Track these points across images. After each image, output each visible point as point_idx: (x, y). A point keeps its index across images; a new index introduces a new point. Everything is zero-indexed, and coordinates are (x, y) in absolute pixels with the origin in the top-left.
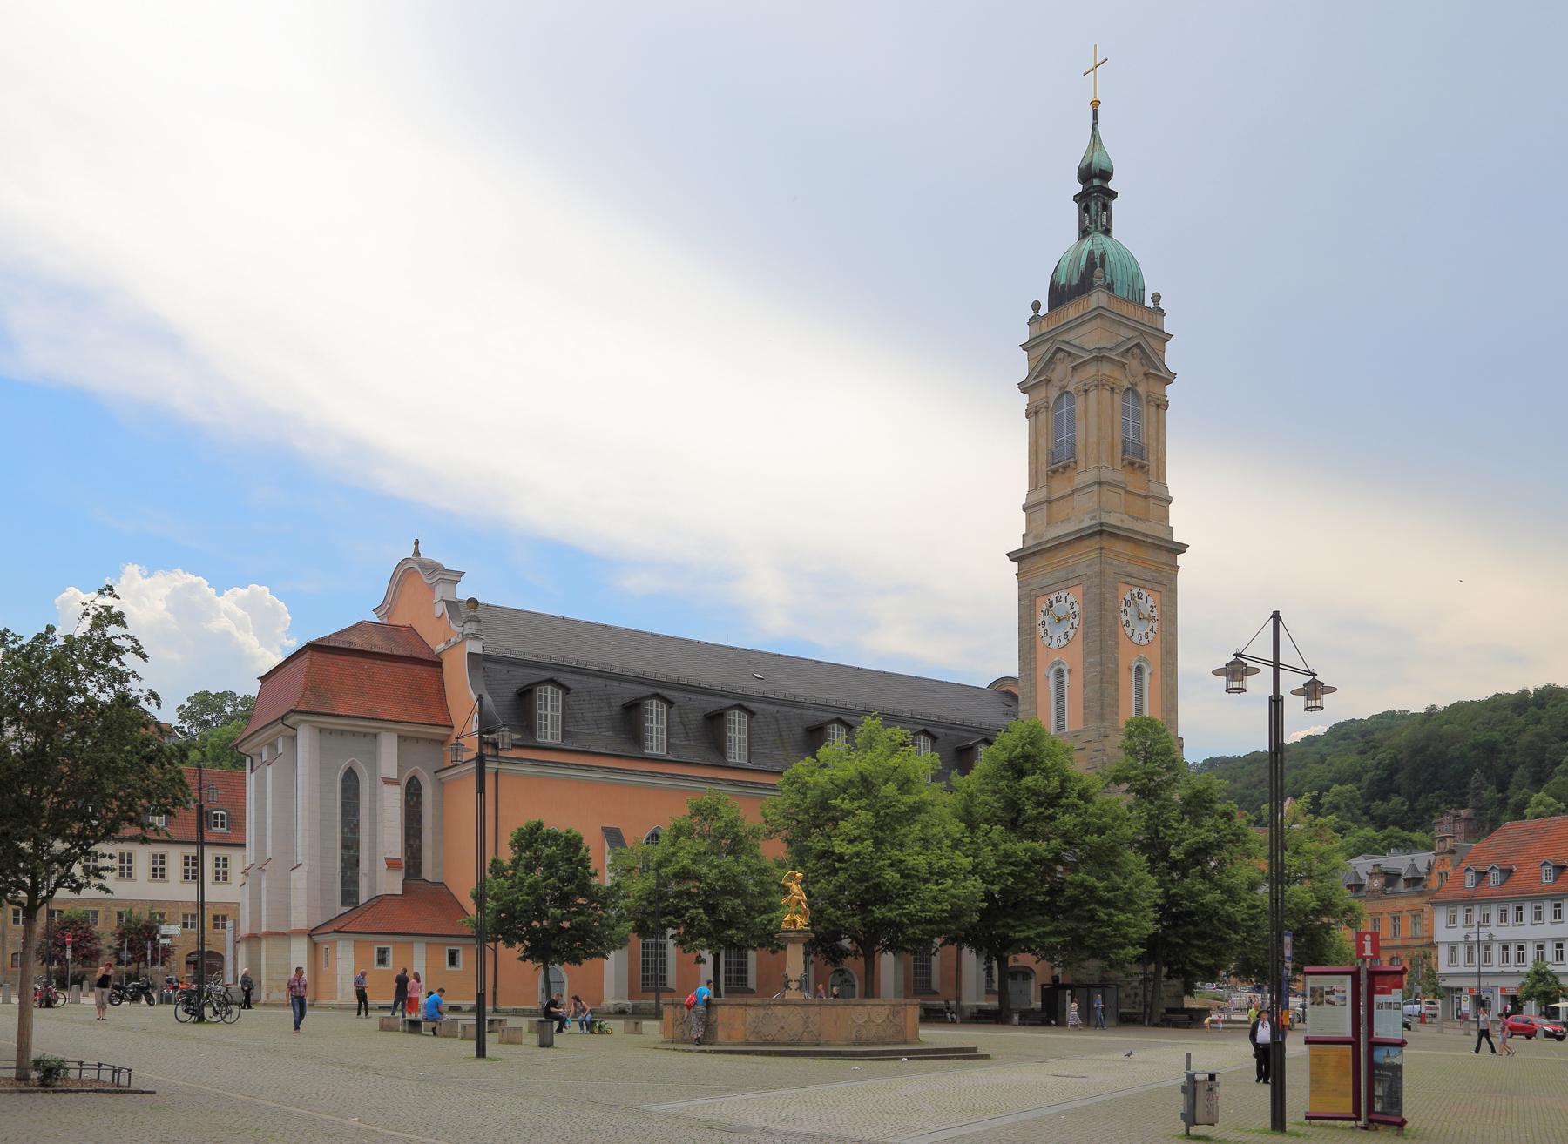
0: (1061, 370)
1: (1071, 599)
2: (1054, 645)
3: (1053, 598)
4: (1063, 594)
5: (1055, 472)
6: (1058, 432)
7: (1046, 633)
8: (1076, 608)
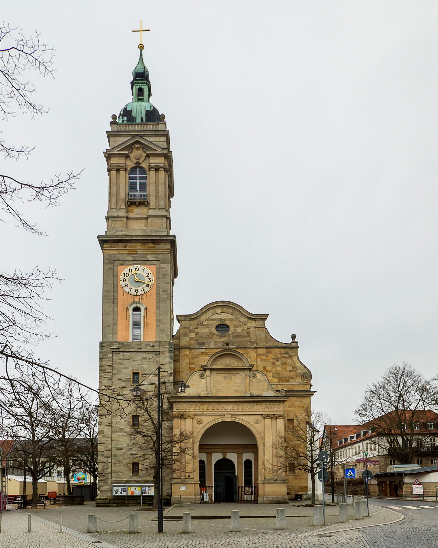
0: (136, 153)
7: (126, 285)
8: (151, 276)
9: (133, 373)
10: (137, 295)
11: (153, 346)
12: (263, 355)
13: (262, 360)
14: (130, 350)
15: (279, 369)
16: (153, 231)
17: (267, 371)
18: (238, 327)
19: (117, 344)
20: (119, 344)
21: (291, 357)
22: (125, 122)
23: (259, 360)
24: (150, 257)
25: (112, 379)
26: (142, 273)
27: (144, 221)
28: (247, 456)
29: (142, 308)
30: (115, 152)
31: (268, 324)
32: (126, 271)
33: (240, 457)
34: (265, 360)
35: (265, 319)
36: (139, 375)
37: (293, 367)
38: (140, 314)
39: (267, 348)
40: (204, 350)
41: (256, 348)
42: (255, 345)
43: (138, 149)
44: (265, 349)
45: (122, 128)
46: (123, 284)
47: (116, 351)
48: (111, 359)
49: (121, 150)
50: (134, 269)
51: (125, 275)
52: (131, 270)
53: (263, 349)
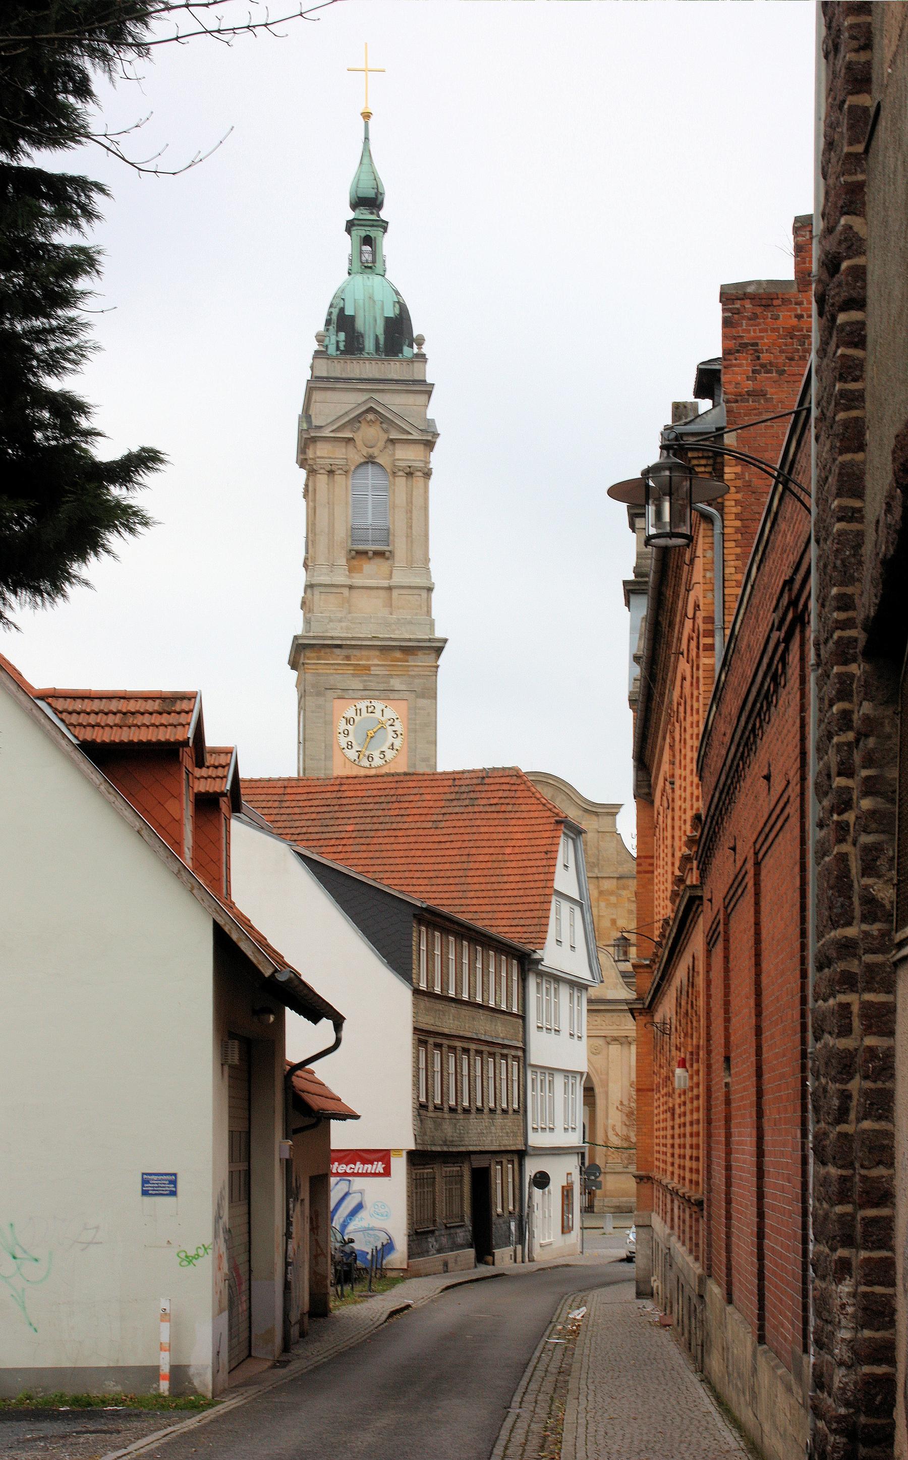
1: (390, 713)
3: (362, 705)
4: (379, 705)
7: (350, 745)
8: (398, 726)
12: (612, 893)
13: (609, 905)
16: (402, 621)
23: (602, 904)
32: (350, 713)
34: (615, 906)
39: (618, 878)
41: (597, 878)
44: (615, 880)
45: (338, 369)
46: (343, 741)
50: (364, 710)
51: (348, 721)
52: (358, 712)
53: (611, 880)
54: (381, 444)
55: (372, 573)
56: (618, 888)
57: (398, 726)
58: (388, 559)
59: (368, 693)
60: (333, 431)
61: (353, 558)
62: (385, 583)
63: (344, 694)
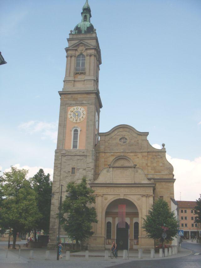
0: (81, 48)
2: (75, 121)
3: (75, 108)
4: (79, 107)
5: (77, 73)
6: (78, 64)
7: (71, 117)
9: (72, 168)
10: (76, 123)
11: (83, 152)
12: (146, 156)
14: (71, 154)
15: (155, 165)
17: (148, 166)
18: (132, 140)
19: (64, 151)
20: (65, 151)
21: (161, 157)
22: (77, 33)
24: (84, 102)
25: (60, 172)
26: (80, 110)
27: (82, 82)
28: (135, 220)
29: (79, 130)
30: (70, 48)
31: (148, 138)
33: (131, 220)
35: (147, 135)
36: (75, 170)
37: (163, 164)
38: (78, 133)
39: (148, 152)
40: (112, 154)
41: (142, 152)
42: (141, 151)
43: (82, 46)
45: (75, 37)
47: (64, 155)
48: (60, 160)
49: (73, 47)
50: (76, 109)
54: (84, 50)
55: (80, 77)
56: (148, 155)
57: (85, 112)
58: (84, 74)
59: (77, 105)
60: (72, 48)
61: (75, 75)
62: (83, 80)
63: (71, 105)
